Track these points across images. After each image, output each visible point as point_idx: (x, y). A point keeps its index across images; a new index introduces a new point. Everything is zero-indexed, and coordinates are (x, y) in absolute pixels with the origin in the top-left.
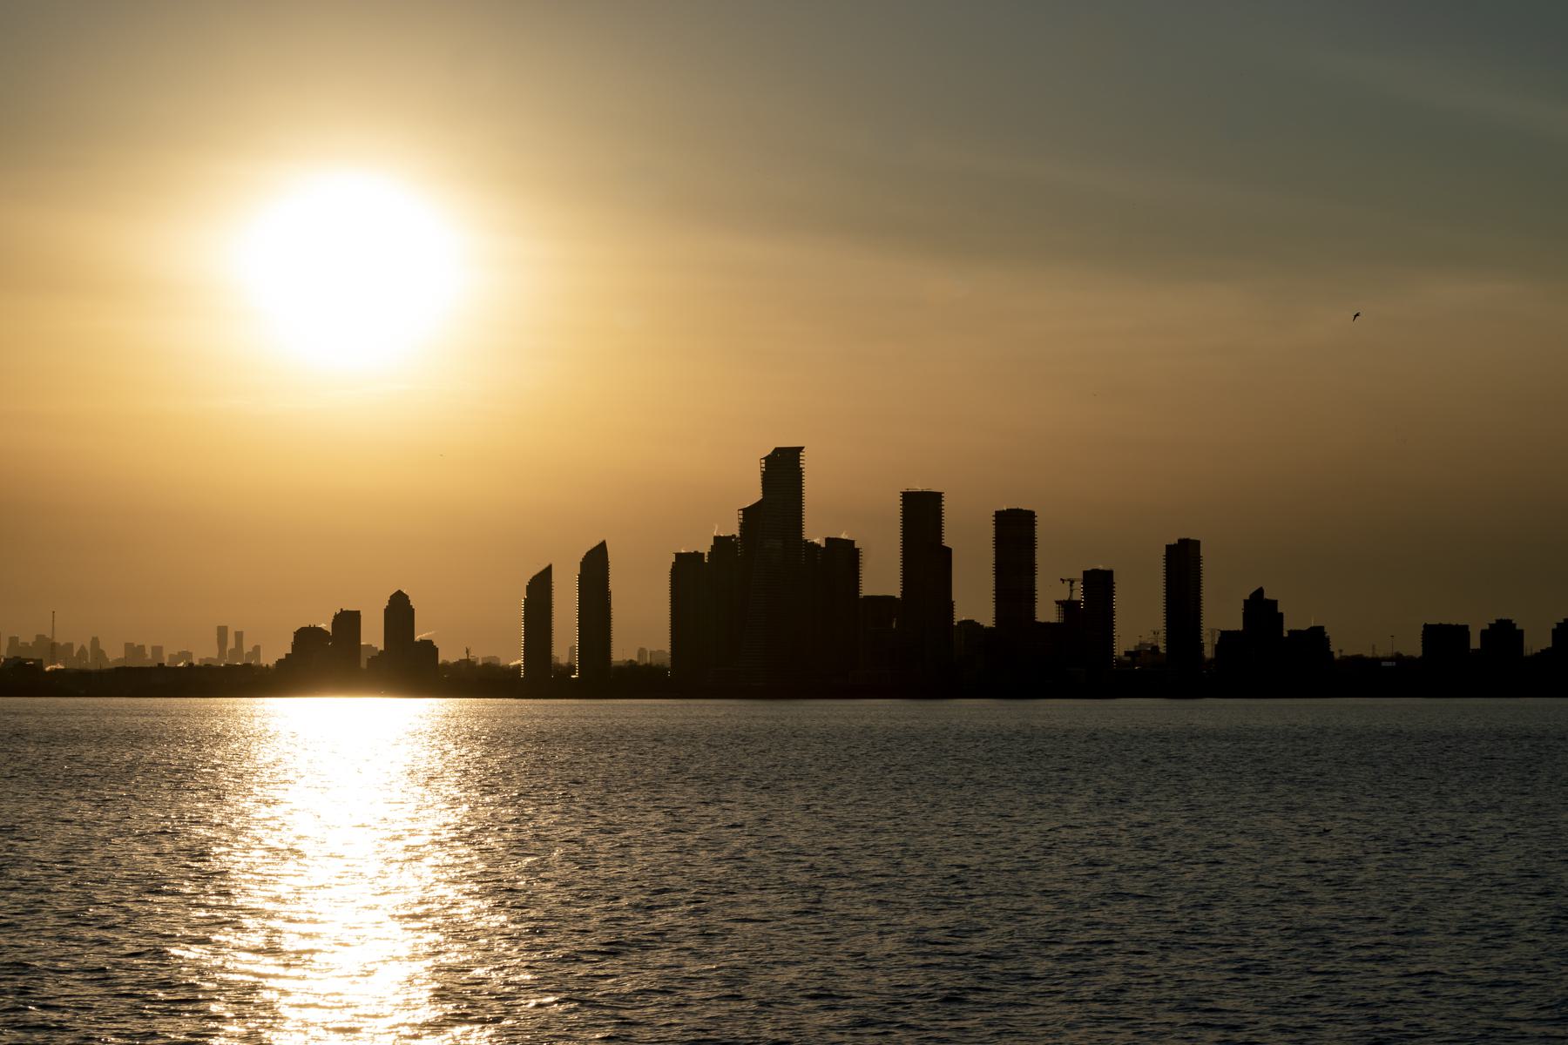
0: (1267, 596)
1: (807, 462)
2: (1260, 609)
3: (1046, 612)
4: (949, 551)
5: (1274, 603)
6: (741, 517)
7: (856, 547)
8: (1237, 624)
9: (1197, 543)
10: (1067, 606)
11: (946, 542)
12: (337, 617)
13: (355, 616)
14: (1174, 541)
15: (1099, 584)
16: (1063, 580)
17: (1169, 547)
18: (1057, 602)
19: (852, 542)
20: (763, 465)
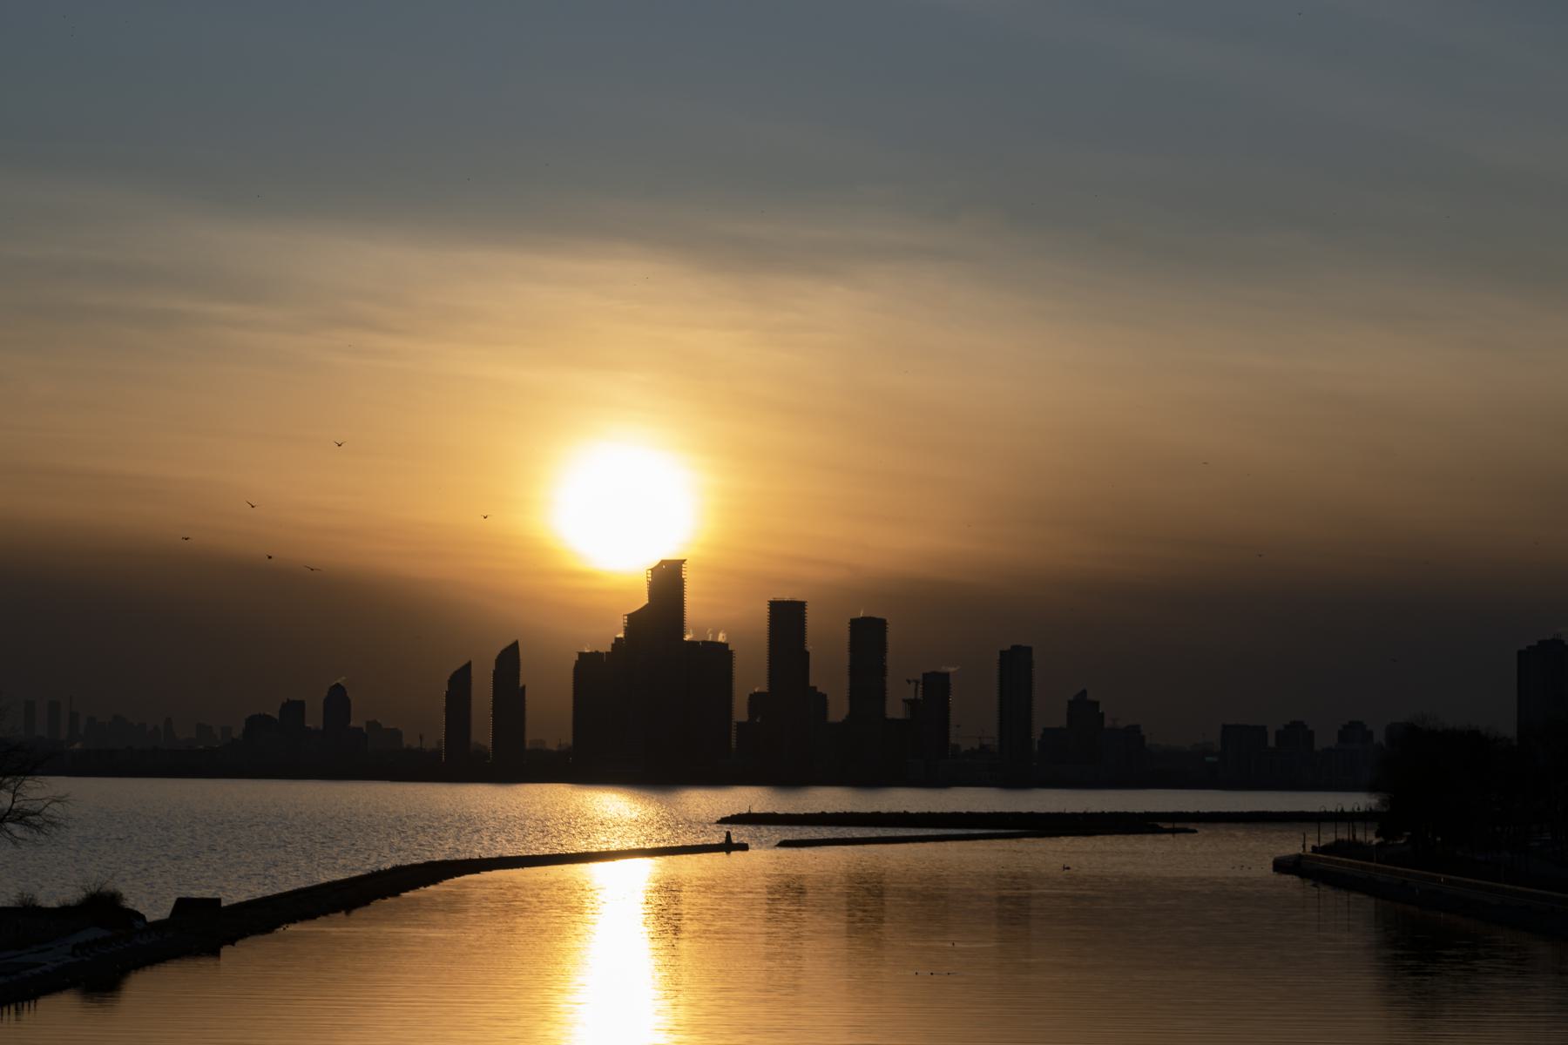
0: (1091, 696)
1: (688, 575)
2: (1083, 709)
3: (895, 709)
4: (808, 653)
5: (1097, 704)
6: (626, 621)
7: (730, 648)
8: (1060, 721)
9: (1029, 650)
10: (911, 704)
11: (809, 647)
12: (284, 706)
13: (301, 704)
14: (1007, 647)
15: (936, 686)
16: (909, 682)
17: (1002, 653)
18: (904, 701)
19: (724, 646)
20: (650, 576)
